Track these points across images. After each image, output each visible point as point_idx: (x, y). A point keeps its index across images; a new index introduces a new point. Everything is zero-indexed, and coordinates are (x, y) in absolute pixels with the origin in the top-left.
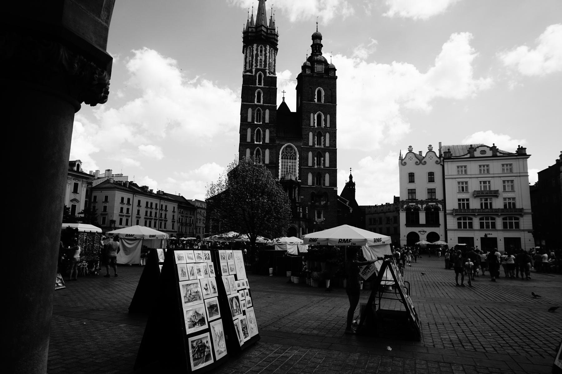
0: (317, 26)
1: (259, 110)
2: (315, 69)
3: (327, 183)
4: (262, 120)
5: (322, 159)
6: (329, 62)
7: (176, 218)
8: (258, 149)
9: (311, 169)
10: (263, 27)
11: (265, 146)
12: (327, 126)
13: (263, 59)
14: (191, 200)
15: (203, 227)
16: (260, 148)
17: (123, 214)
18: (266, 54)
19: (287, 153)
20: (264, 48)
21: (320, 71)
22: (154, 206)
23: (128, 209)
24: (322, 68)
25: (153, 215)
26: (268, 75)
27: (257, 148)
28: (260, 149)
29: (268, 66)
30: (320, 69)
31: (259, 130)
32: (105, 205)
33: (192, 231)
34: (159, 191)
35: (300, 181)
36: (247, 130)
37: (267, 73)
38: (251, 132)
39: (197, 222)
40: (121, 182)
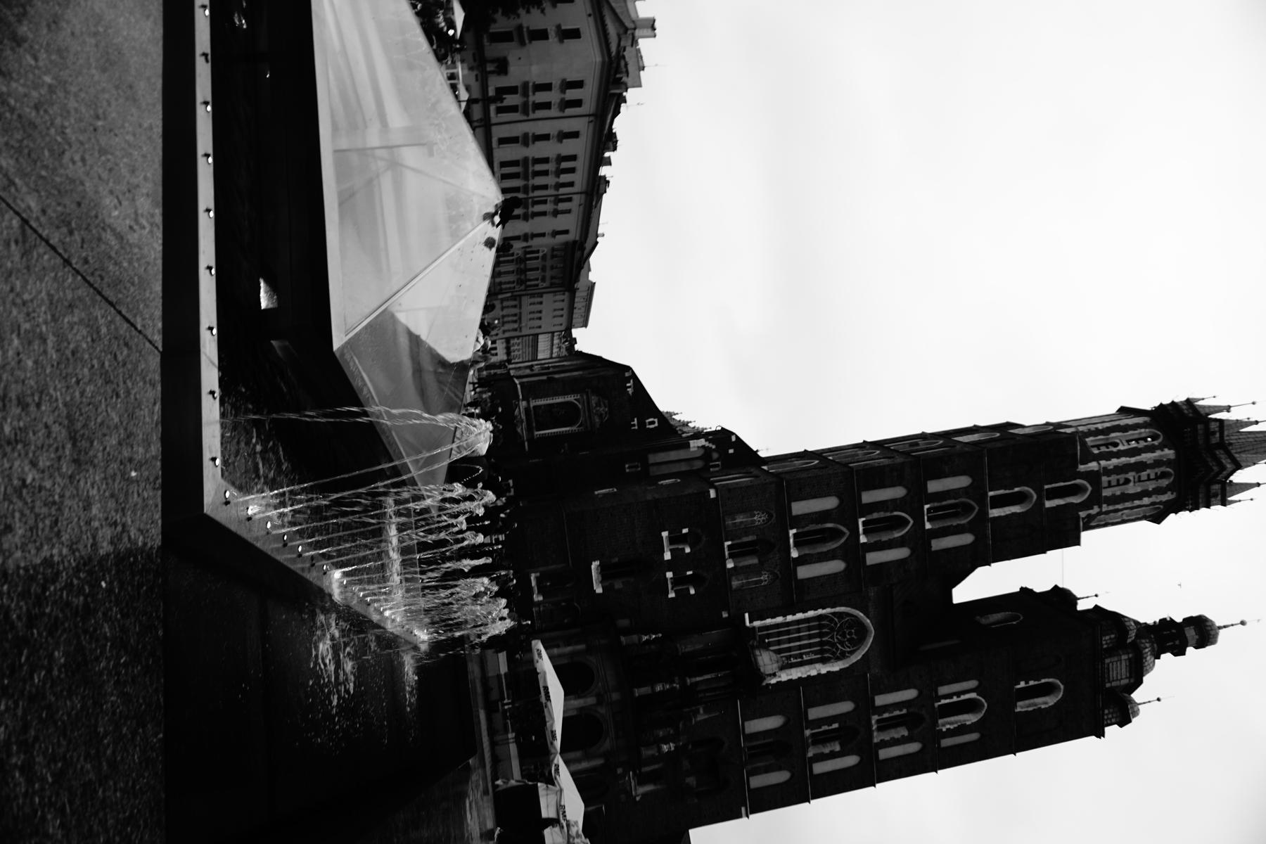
0: (1232, 625)
2: (1116, 659)
3: (757, 782)
4: (937, 526)
5: (837, 748)
6: (1137, 696)
7: (536, 242)
9: (797, 720)
11: (853, 553)
12: (944, 738)
13: (1132, 489)
14: (589, 270)
15: (520, 313)
16: (846, 540)
17: (531, 93)
21: (1111, 673)
22: (565, 178)
23: (547, 106)
24: (1119, 678)
25: (539, 181)
26: (1082, 514)
27: (844, 529)
28: (843, 540)
29: (1111, 508)
30: (1115, 672)
31: (906, 522)
32: (552, 34)
33: (506, 289)
34: (608, 182)
38: (894, 501)
39: (532, 296)
40: (624, 70)
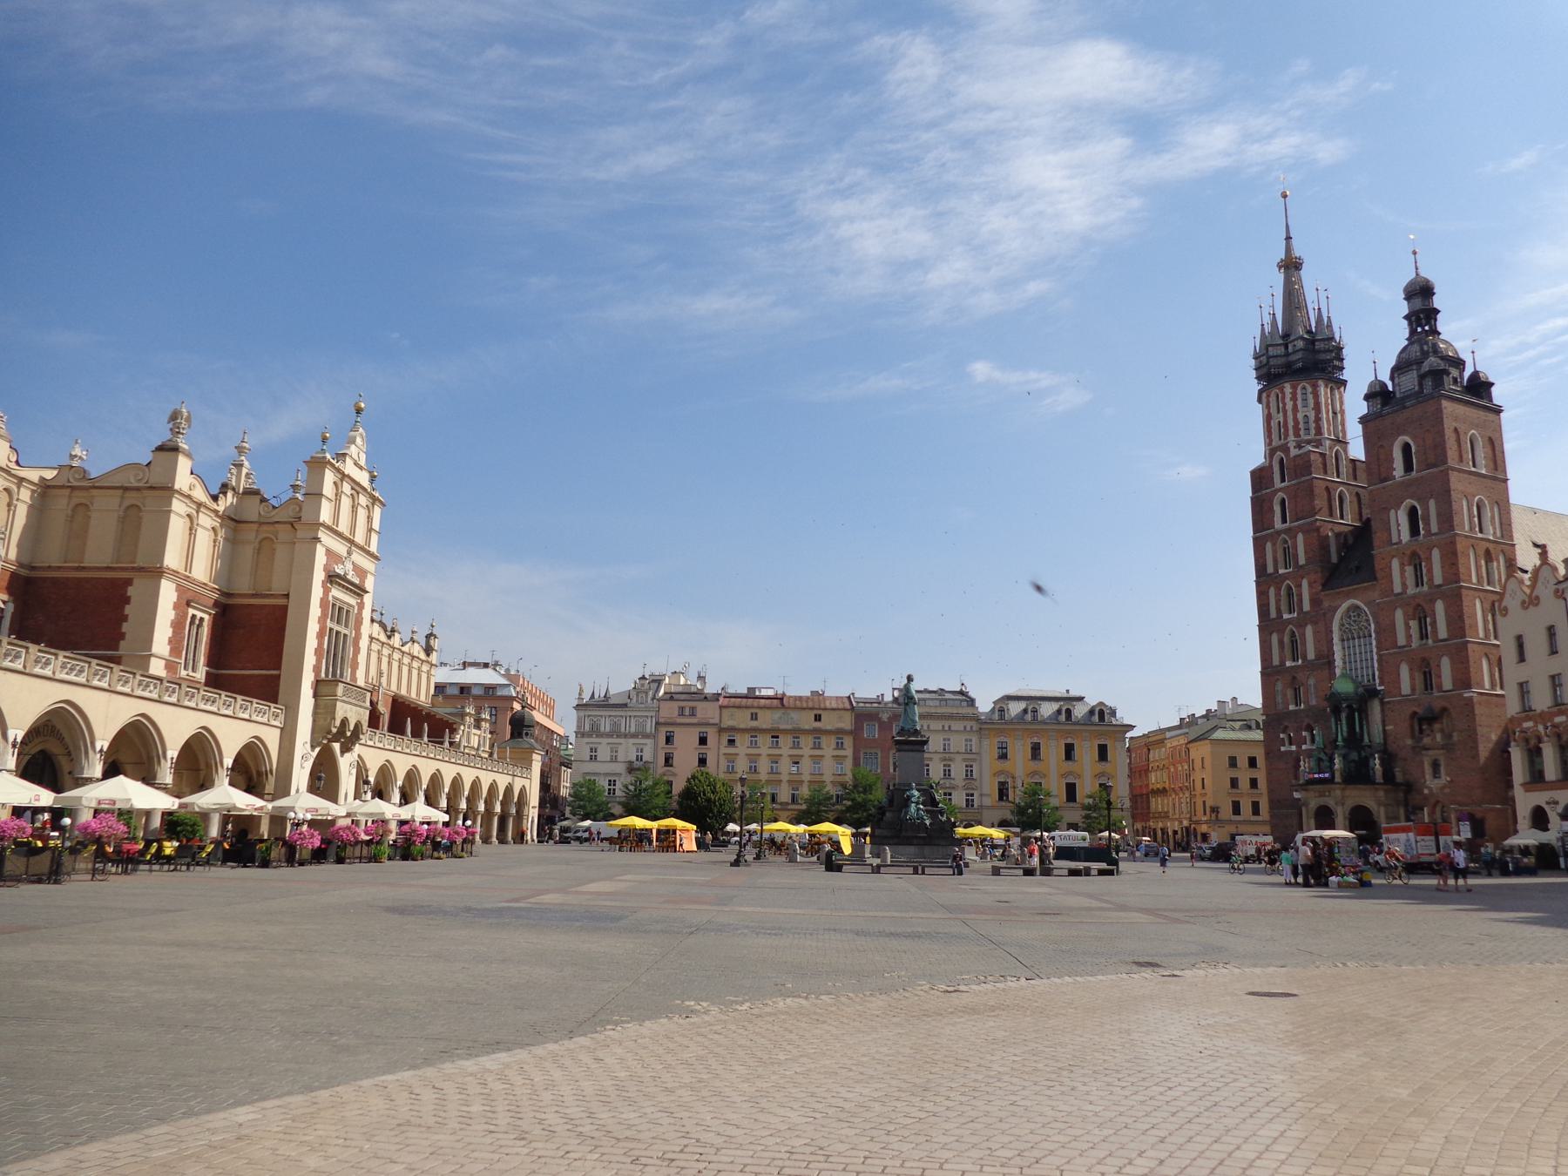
1: (1286, 542)
3: (1447, 683)
8: (1291, 630)
10: (1270, 349)
12: (1430, 530)
18: (1284, 404)
19: (1349, 624)
20: (1280, 395)
26: (1294, 452)
27: (1289, 628)
29: (1291, 432)
30: (1409, 384)
35: (1383, 688)
36: (1268, 592)
37: (1292, 449)
38: (1276, 595)
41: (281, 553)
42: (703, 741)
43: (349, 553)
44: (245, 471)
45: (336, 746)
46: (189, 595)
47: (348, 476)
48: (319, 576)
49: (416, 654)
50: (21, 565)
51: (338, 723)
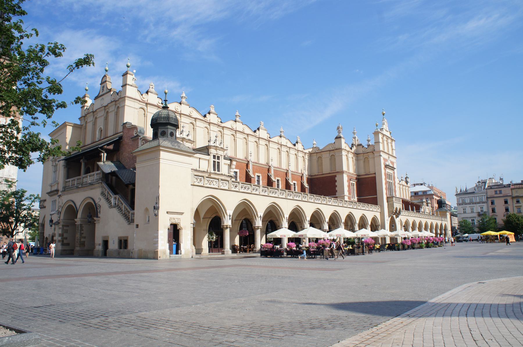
41: (371, 161)
42: (506, 202)
43: (389, 158)
44: (356, 139)
45: (394, 216)
46: (350, 178)
47: (385, 135)
48: (383, 166)
49: (404, 184)
50: (309, 176)
51: (395, 209)
